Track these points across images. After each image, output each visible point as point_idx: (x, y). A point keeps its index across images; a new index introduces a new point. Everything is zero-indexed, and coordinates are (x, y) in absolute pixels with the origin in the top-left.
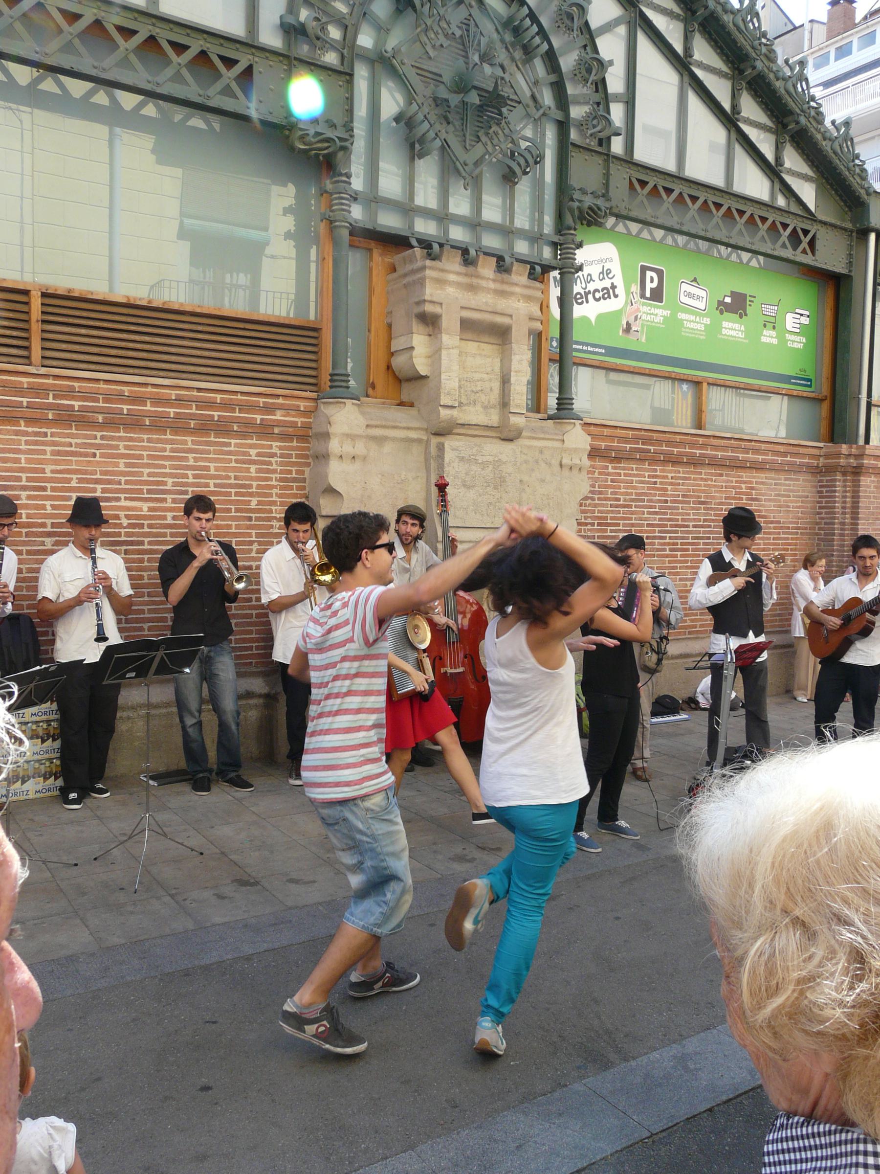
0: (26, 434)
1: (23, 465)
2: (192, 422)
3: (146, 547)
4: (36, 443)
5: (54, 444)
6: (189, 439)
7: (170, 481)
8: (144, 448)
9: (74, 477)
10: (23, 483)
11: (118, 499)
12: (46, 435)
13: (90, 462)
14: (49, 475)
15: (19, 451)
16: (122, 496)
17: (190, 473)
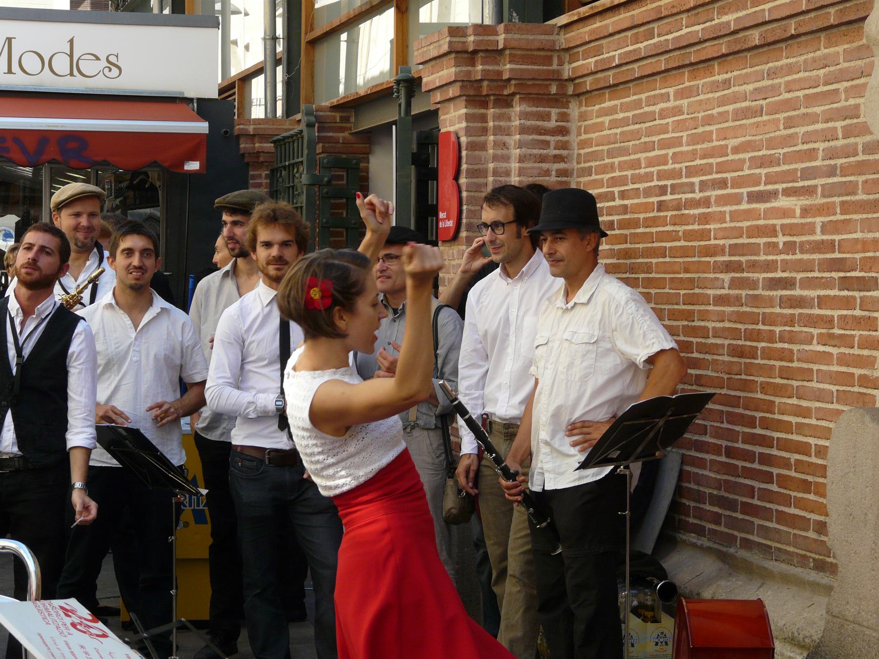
0: (715, 87)
1: (715, 143)
2: (832, 10)
3: (798, 292)
4: (723, 102)
5: (735, 98)
6: (840, 49)
7: (821, 146)
8: (801, 85)
9: (747, 156)
10: (715, 176)
11: (774, 194)
12: (727, 84)
13: (757, 125)
14: (731, 157)
15: (709, 120)
16: (780, 187)
17: (839, 124)
